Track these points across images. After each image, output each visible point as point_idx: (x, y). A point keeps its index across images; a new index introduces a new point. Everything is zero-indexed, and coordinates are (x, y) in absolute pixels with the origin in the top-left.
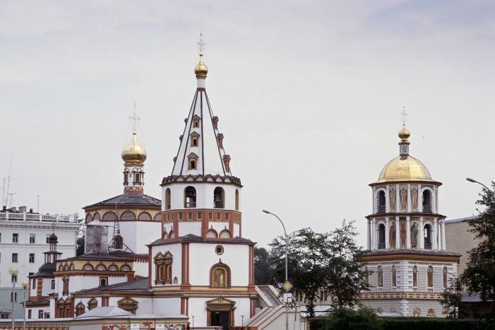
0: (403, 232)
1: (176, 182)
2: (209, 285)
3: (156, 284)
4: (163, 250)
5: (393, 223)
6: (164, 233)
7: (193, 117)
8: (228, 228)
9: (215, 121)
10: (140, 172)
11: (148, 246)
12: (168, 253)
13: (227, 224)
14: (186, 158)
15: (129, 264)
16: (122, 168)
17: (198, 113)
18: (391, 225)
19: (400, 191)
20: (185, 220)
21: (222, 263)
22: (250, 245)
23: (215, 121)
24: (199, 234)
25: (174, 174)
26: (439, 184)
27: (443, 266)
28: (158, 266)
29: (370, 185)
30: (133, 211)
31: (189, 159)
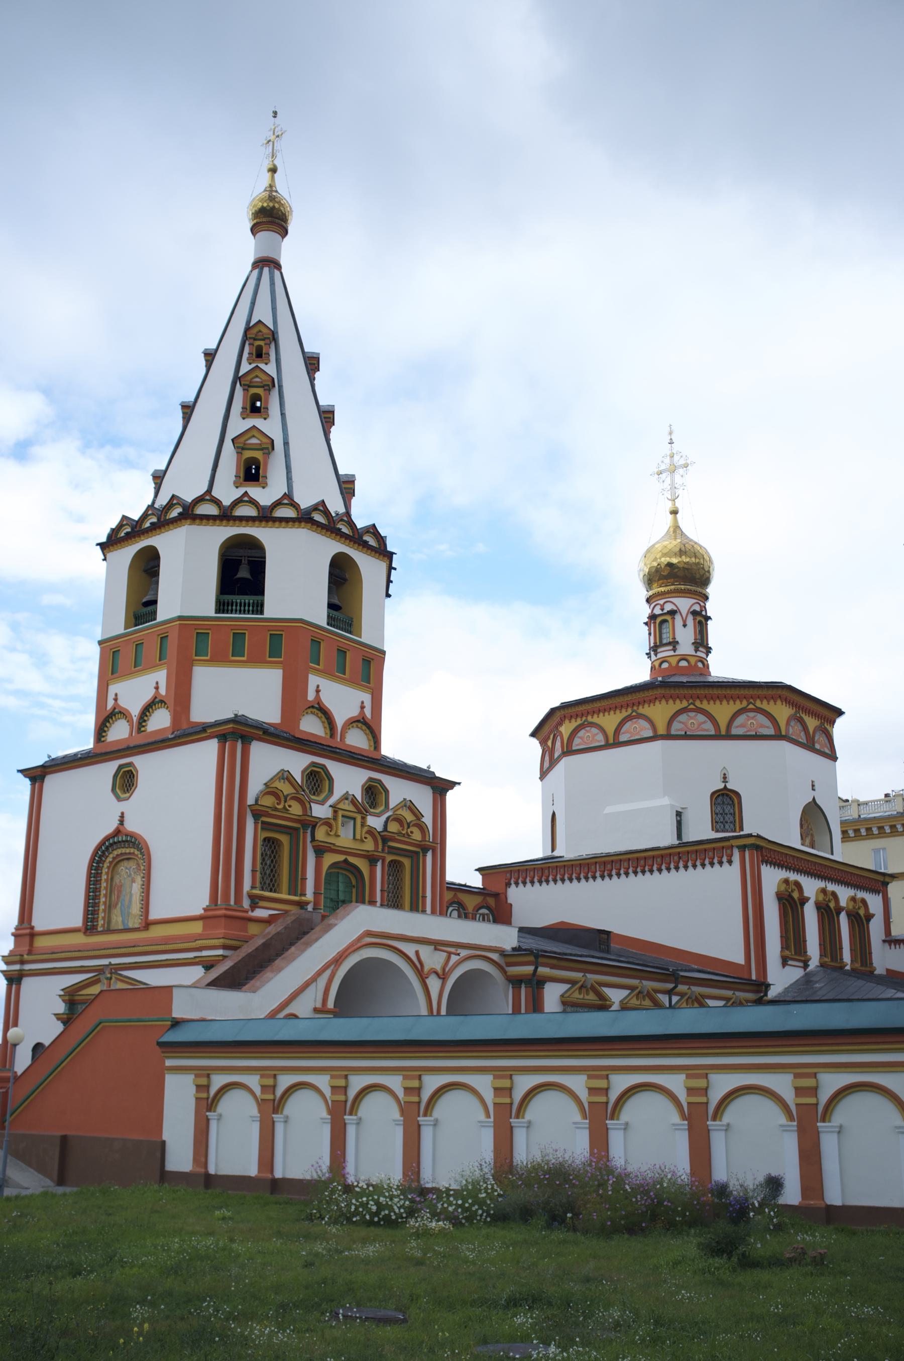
7: (248, 329)
8: (368, 713)
13: (367, 698)
14: (228, 445)
17: (263, 314)
20: (219, 659)
23: (312, 363)
24: (268, 710)
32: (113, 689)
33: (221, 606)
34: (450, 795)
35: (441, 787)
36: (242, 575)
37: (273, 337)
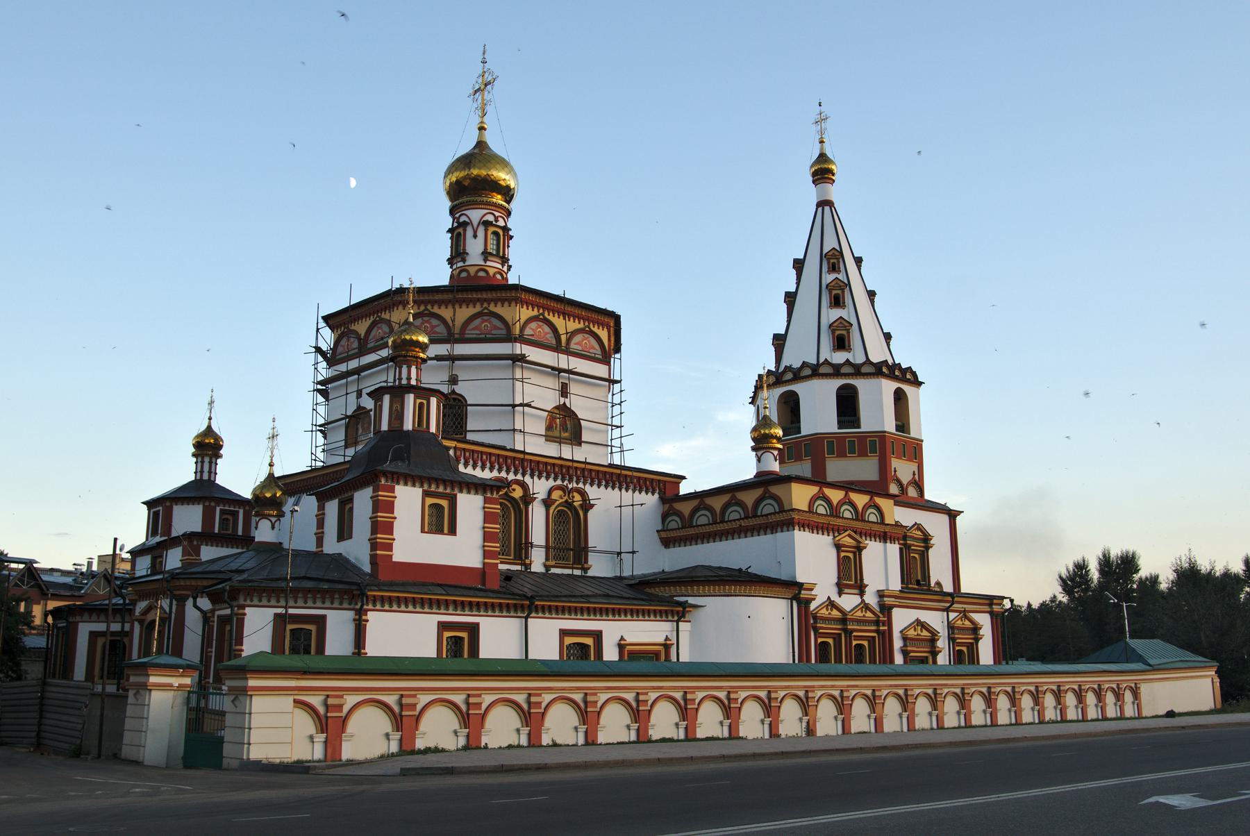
9: (858, 261)
20: (842, 454)
23: (858, 261)
31: (833, 332)
33: (841, 424)
34: (958, 518)
35: (953, 515)
36: (847, 405)
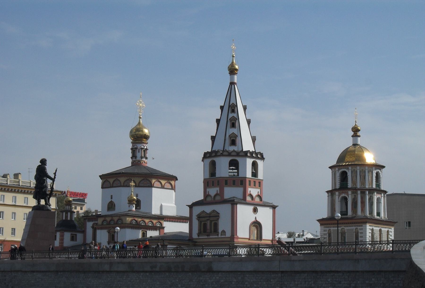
0: (363, 203)
1: (222, 155)
2: (248, 237)
3: (198, 236)
4: (208, 209)
5: (355, 196)
6: (206, 195)
8: (259, 193)
9: (245, 108)
10: (146, 149)
11: (188, 206)
12: (214, 211)
13: (259, 190)
15: (162, 221)
16: (130, 146)
18: (353, 197)
19: (360, 172)
20: (230, 186)
21: (257, 221)
22: (273, 208)
25: (216, 148)
26: (383, 167)
27: (387, 230)
28: (200, 222)
29: (330, 168)
30: (150, 179)
32: (208, 190)
37: (237, 106)
